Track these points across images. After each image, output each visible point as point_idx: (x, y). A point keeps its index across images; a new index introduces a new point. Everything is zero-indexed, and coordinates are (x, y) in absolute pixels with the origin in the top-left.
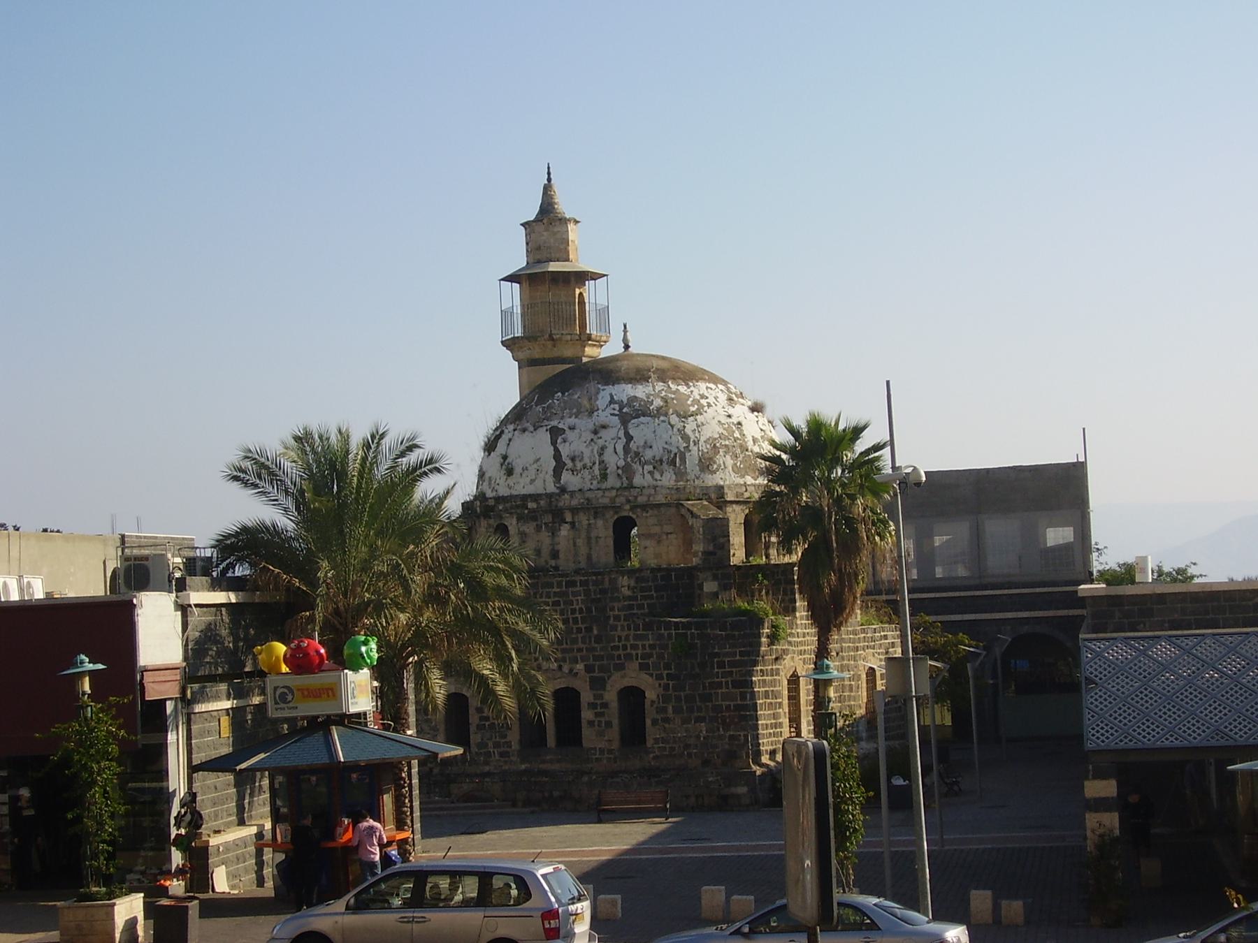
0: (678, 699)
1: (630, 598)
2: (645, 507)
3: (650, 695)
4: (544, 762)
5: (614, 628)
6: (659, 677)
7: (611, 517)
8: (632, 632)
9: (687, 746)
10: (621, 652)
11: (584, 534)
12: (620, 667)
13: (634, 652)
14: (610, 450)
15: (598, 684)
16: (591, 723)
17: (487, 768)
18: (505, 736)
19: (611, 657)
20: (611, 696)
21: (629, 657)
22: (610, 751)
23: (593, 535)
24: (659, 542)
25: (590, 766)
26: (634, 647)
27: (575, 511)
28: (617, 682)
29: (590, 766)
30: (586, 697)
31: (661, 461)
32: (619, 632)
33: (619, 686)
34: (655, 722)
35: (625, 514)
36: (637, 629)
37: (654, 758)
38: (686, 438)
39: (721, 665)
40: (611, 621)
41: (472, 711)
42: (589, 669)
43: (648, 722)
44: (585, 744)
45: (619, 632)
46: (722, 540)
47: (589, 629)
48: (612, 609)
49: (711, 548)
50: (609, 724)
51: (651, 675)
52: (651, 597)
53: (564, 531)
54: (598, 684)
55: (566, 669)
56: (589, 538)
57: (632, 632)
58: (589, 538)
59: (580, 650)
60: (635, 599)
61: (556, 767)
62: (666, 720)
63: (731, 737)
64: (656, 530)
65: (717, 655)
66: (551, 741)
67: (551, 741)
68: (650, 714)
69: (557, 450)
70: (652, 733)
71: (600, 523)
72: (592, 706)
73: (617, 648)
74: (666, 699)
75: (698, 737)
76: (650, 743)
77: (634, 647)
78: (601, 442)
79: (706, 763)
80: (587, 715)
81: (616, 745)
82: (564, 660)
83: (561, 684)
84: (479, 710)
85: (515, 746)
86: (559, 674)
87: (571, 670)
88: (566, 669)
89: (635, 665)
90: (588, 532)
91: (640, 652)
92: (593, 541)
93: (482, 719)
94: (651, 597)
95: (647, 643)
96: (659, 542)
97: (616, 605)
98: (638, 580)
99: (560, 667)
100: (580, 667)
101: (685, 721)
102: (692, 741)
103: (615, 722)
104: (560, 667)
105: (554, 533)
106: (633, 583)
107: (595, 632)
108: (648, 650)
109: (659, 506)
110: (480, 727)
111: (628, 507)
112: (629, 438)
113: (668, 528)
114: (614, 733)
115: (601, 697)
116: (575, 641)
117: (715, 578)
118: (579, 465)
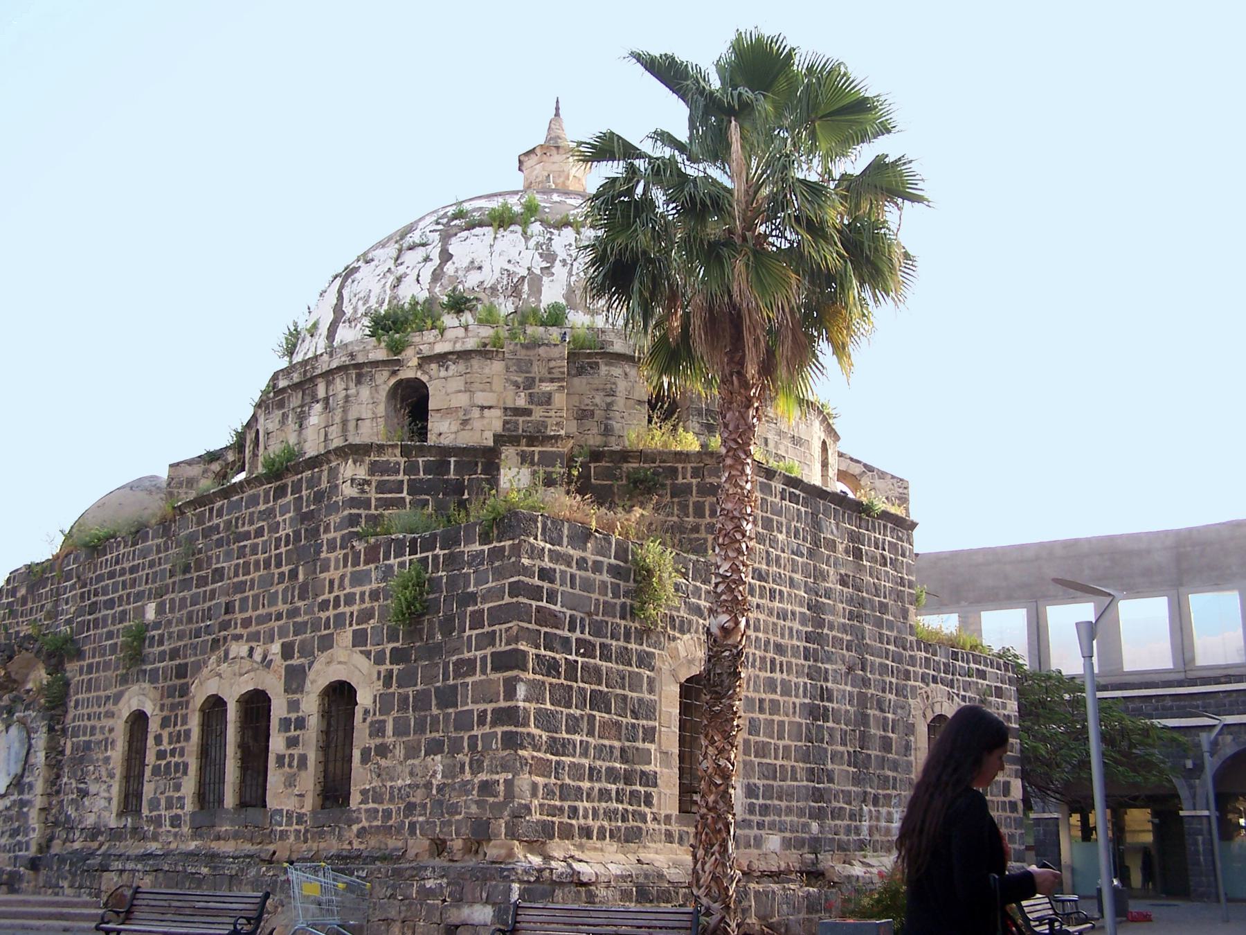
0: (404, 699)
1: (353, 502)
2: (441, 358)
3: (364, 698)
4: (218, 838)
5: (325, 568)
6: (379, 660)
7: (385, 382)
8: (350, 569)
9: (410, 808)
10: (331, 613)
11: (338, 419)
12: (327, 643)
13: (347, 610)
14: (409, 281)
15: (295, 679)
16: (280, 759)
17: (153, 847)
18: (178, 787)
19: (316, 626)
20: (310, 705)
21: (340, 621)
22: (300, 819)
23: (352, 415)
24: (465, 422)
25: (272, 847)
26: (350, 599)
27: (329, 375)
28: (322, 674)
29: (272, 847)
30: (278, 709)
31: (493, 289)
32: (334, 574)
33: (323, 683)
34: (365, 757)
35: (407, 374)
36: (356, 563)
37: (362, 833)
38: (550, 257)
39: (477, 622)
40: (323, 555)
41: (150, 741)
42: (287, 652)
43: (357, 754)
44: (272, 803)
45: (334, 574)
46: (547, 387)
47: (294, 574)
48: (327, 530)
49: (521, 402)
50: (303, 760)
51: (367, 654)
52: (400, 503)
53: (315, 417)
54: (295, 679)
55: (258, 656)
56: (345, 422)
57: (350, 569)
58: (345, 422)
59: (279, 617)
60: (366, 504)
61: (228, 847)
62: (383, 751)
63: (486, 788)
64: (462, 400)
65: (472, 598)
66: (230, 800)
67: (230, 800)
68: (362, 737)
69: (340, 297)
70: (361, 777)
71: (365, 392)
72: (285, 724)
73: (324, 606)
74: (384, 703)
75: (428, 785)
76: (355, 800)
77: (350, 599)
78: (401, 270)
79: (439, 847)
80: (277, 743)
81: (308, 805)
82: (255, 637)
83: (246, 685)
84: (158, 740)
85: (189, 806)
86: (247, 664)
87: (265, 657)
88: (258, 656)
89: (345, 637)
90: (345, 411)
91: (355, 608)
92: (351, 425)
93: (161, 755)
94: (400, 503)
95: (367, 588)
96: (465, 422)
97: (334, 519)
98: (374, 468)
99: (251, 650)
100: (276, 648)
101: (412, 752)
102: (418, 797)
103: (312, 757)
104: (251, 650)
105: (301, 419)
106: (361, 473)
107: (301, 577)
108: (367, 605)
109: (465, 355)
110: (156, 771)
111: (414, 362)
112: (446, 256)
113: (482, 398)
114: (308, 781)
115: (294, 706)
116: (273, 600)
117: (525, 459)
118: (362, 310)
